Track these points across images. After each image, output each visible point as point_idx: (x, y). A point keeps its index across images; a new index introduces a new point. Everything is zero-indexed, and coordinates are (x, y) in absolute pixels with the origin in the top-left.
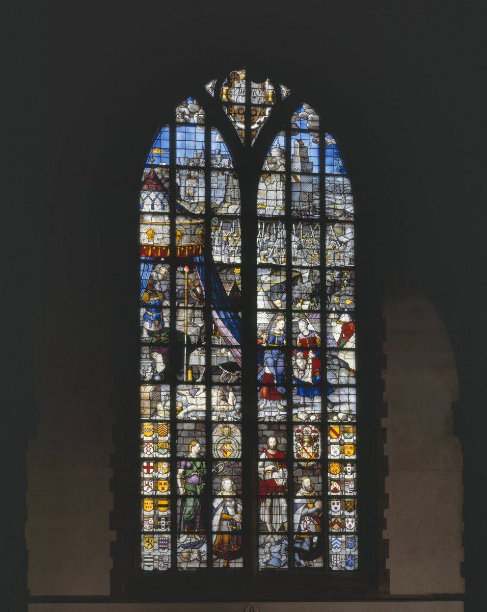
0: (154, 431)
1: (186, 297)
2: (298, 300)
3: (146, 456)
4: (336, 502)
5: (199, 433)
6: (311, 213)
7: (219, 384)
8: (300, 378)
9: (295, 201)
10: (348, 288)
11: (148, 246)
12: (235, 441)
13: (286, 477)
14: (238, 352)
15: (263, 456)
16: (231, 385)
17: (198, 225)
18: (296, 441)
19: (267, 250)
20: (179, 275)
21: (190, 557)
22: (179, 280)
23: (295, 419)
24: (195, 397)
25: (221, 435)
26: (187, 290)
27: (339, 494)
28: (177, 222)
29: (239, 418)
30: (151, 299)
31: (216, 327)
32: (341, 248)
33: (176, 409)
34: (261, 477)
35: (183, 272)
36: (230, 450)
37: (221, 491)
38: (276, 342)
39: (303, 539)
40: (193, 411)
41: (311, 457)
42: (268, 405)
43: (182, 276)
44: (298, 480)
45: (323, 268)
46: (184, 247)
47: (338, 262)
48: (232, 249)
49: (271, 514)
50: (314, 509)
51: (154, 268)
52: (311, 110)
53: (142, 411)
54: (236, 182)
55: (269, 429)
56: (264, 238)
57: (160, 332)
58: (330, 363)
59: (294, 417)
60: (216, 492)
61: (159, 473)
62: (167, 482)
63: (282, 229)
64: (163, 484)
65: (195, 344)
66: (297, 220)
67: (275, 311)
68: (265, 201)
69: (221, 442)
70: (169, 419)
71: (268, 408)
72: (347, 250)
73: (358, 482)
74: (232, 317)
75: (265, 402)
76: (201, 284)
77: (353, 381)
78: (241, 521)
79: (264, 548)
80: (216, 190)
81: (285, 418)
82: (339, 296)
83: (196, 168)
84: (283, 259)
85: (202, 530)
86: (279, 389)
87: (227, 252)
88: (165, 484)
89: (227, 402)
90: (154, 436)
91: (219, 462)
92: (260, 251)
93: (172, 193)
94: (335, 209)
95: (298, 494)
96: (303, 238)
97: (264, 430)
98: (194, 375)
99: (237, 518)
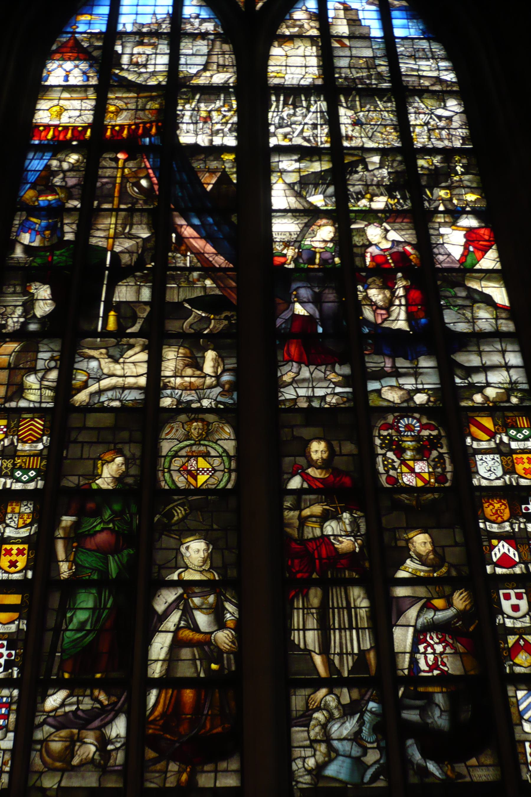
1: (116, 194)
2: (360, 196)
4: (512, 592)
5: (125, 435)
6: (374, 82)
8: (379, 321)
9: (341, 68)
10: (467, 177)
11: (47, 127)
12: (220, 450)
13: (363, 530)
15: (295, 483)
18: (382, 448)
19: (291, 127)
21: (73, 757)
22: (105, 170)
23: (374, 402)
24: (121, 360)
25: (182, 437)
26: (121, 184)
28: (111, 96)
29: (231, 402)
30: (41, 199)
32: (442, 124)
33: (71, 384)
35: (117, 160)
36: (204, 471)
37: (177, 568)
38: (317, 261)
39: (429, 697)
40: (113, 388)
41: (426, 482)
42: (305, 373)
43: (113, 164)
44: (396, 540)
46: (122, 127)
47: (439, 142)
48: (218, 127)
50: (450, 613)
56: (282, 112)
57: (51, 249)
58: (448, 294)
59: (373, 397)
60: (163, 572)
61: (8, 526)
62: (26, 546)
63: (319, 100)
64: (14, 552)
68: (284, 68)
69: (183, 453)
70: (51, 405)
71: (304, 380)
72: (452, 127)
75: (295, 370)
76: (152, 175)
77: (506, 326)
78: (235, 648)
79: (307, 725)
80: (189, 57)
81: (349, 400)
84: (324, 139)
85: (115, 675)
87: (209, 131)
88: (20, 552)
89: (201, 369)
90: (6, 442)
91: (176, 497)
92: (276, 128)
94: (420, 77)
95: (401, 574)
96: (361, 111)
97: (295, 426)
98: (121, 320)
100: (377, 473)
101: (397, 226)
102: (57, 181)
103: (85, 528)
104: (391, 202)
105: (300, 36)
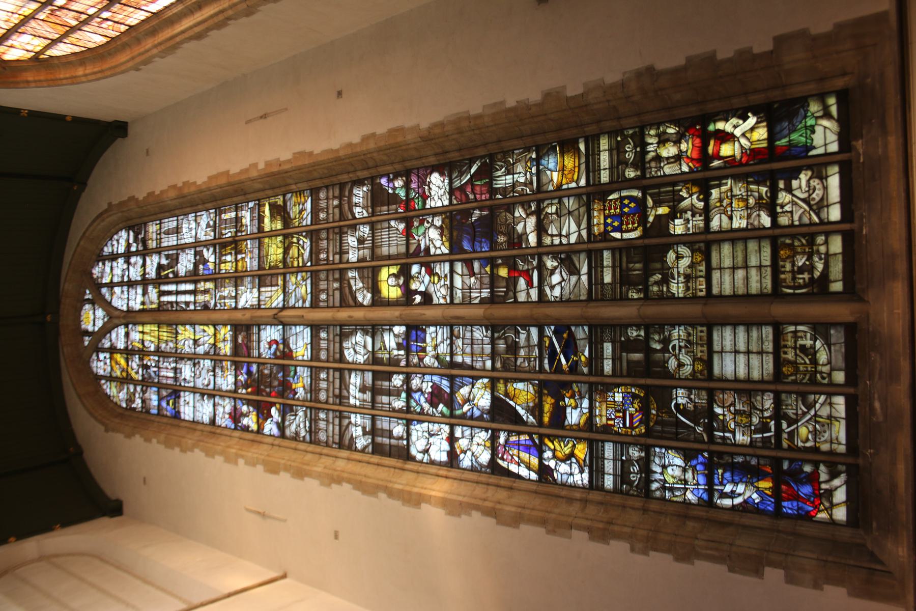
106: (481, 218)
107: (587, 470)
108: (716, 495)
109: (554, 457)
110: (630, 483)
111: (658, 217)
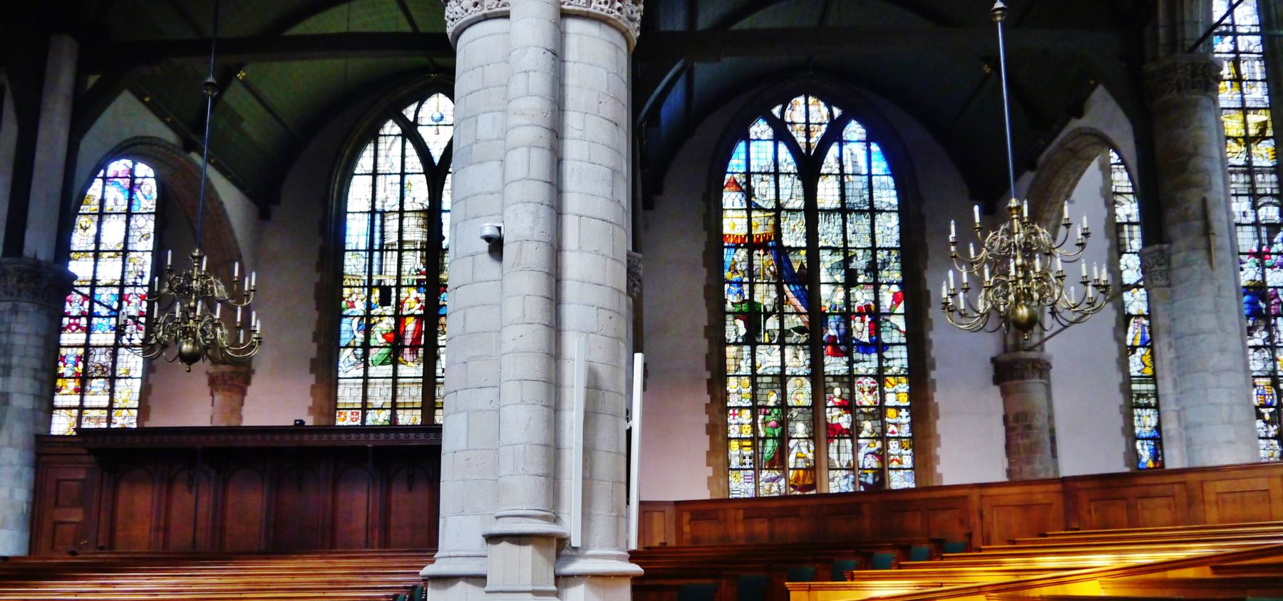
0: (739, 384)
3: (732, 405)
5: (776, 385)
6: (862, 205)
7: (791, 344)
10: (896, 264)
11: (730, 235)
14: (806, 318)
16: (801, 345)
17: (770, 217)
20: (755, 257)
27: (896, 435)
31: (787, 297)
32: (889, 232)
34: (829, 421)
35: (759, 255)
39: (867, 474)
45: (874, 249)
46: (760, 235)
48: (798, 235)
49: (839, 452)
51: (735, 252)
52: (860, 125)
53: (728, 368)
54: (800, 183)
55: (834, 381)
57: (741, 303)
58: (882, 325)
59: (855, 370)
65: (770, 312)
66: (851, 211)
67: (836, 284)
73: (912, 424)
74: (800, 290)
77: (903, 340)
82: (888, 270)
83: (767, 173)
86: (842, 348)
90: (738, 388)
93: (749, 193)
94: (882, 202)
95: (861, 436)
99: (810, 456)
100: (855, 400)
101: (867, 291)
102: (738, 267)
103: (766, 420)
104: (866, 278)
105: (831, 174)
106: (1261, 309)
107: (1140, 374)
108: (1142, 442)
109: (1143, 355)
110: (1138, 398)
111: (1263, 414)
